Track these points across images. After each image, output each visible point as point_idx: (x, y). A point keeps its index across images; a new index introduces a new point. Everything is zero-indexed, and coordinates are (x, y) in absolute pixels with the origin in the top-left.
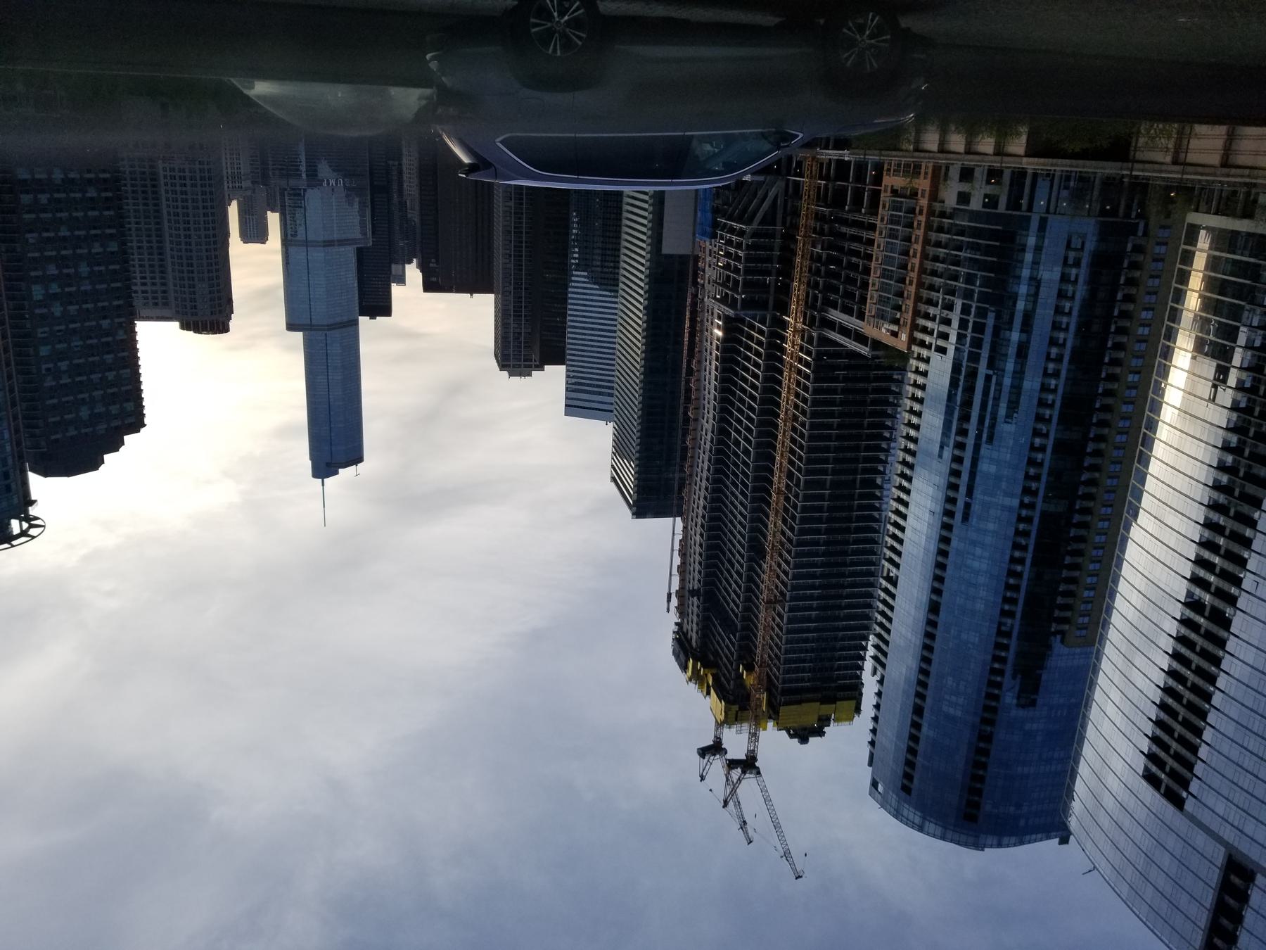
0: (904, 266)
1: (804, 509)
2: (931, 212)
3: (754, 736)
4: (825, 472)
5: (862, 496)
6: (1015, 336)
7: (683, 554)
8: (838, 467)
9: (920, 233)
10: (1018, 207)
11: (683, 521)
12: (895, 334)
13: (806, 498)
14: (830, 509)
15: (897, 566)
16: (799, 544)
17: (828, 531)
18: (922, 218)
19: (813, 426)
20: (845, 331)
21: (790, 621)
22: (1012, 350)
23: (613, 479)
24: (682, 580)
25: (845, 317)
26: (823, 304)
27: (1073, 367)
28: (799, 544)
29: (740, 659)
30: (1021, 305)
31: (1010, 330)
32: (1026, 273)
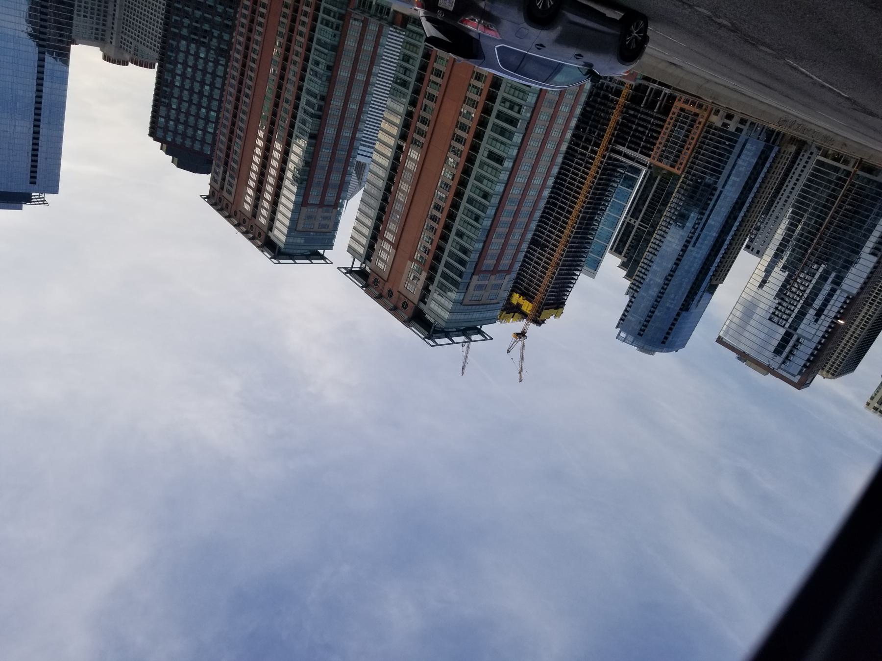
0: (685, 142)
1: (578, 228)
2: (704, 125)
3: (527, 325)
4: (587, 213)
9: (698, 132)
13: (580, 223)
14: (584, 229)
15: (654, 254)
16: (572, 242)
17: (581, 238)
18: (701, 126)
19: (593, 193)
20: (626, 156)
21: (559, 275)
28: (572, 242)
29: (513, 291)
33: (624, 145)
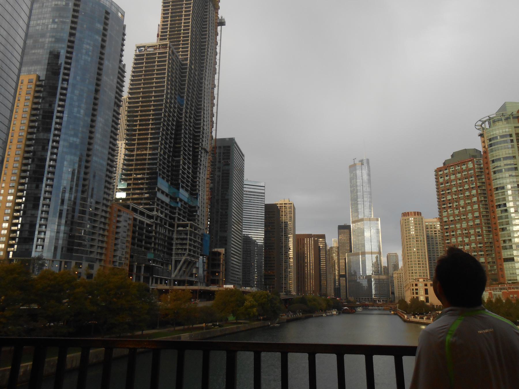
5: (134, 145)
6: (65, 207)
7: (212, 122)
8: (144, 157)
10: (66, 263)
11: (212, 137)
12: (119, 211)
22: (66, 202)
23: (243, 156)
24: (212, 111)
25: (142, 219)
26: (153, 226)
27: (39, 195)
30: (63, 221)
31: (68, 210)
32: (61, 235)
33: (147, 224)
